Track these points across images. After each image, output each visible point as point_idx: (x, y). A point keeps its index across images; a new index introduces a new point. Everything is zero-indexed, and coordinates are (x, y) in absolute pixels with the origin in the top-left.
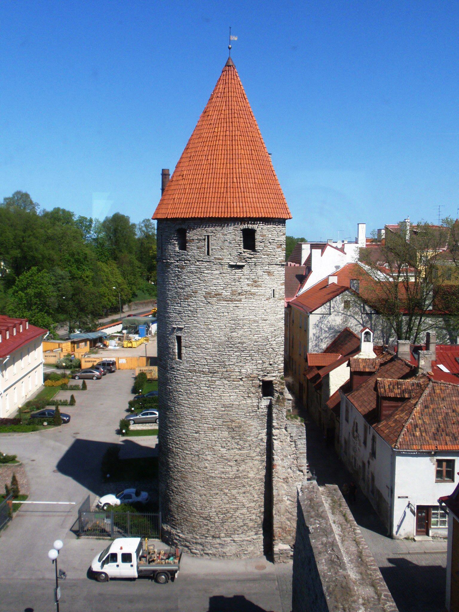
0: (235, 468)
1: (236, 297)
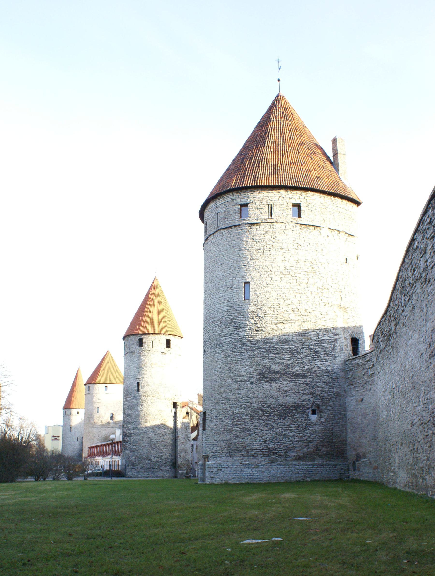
0: (162, 437)
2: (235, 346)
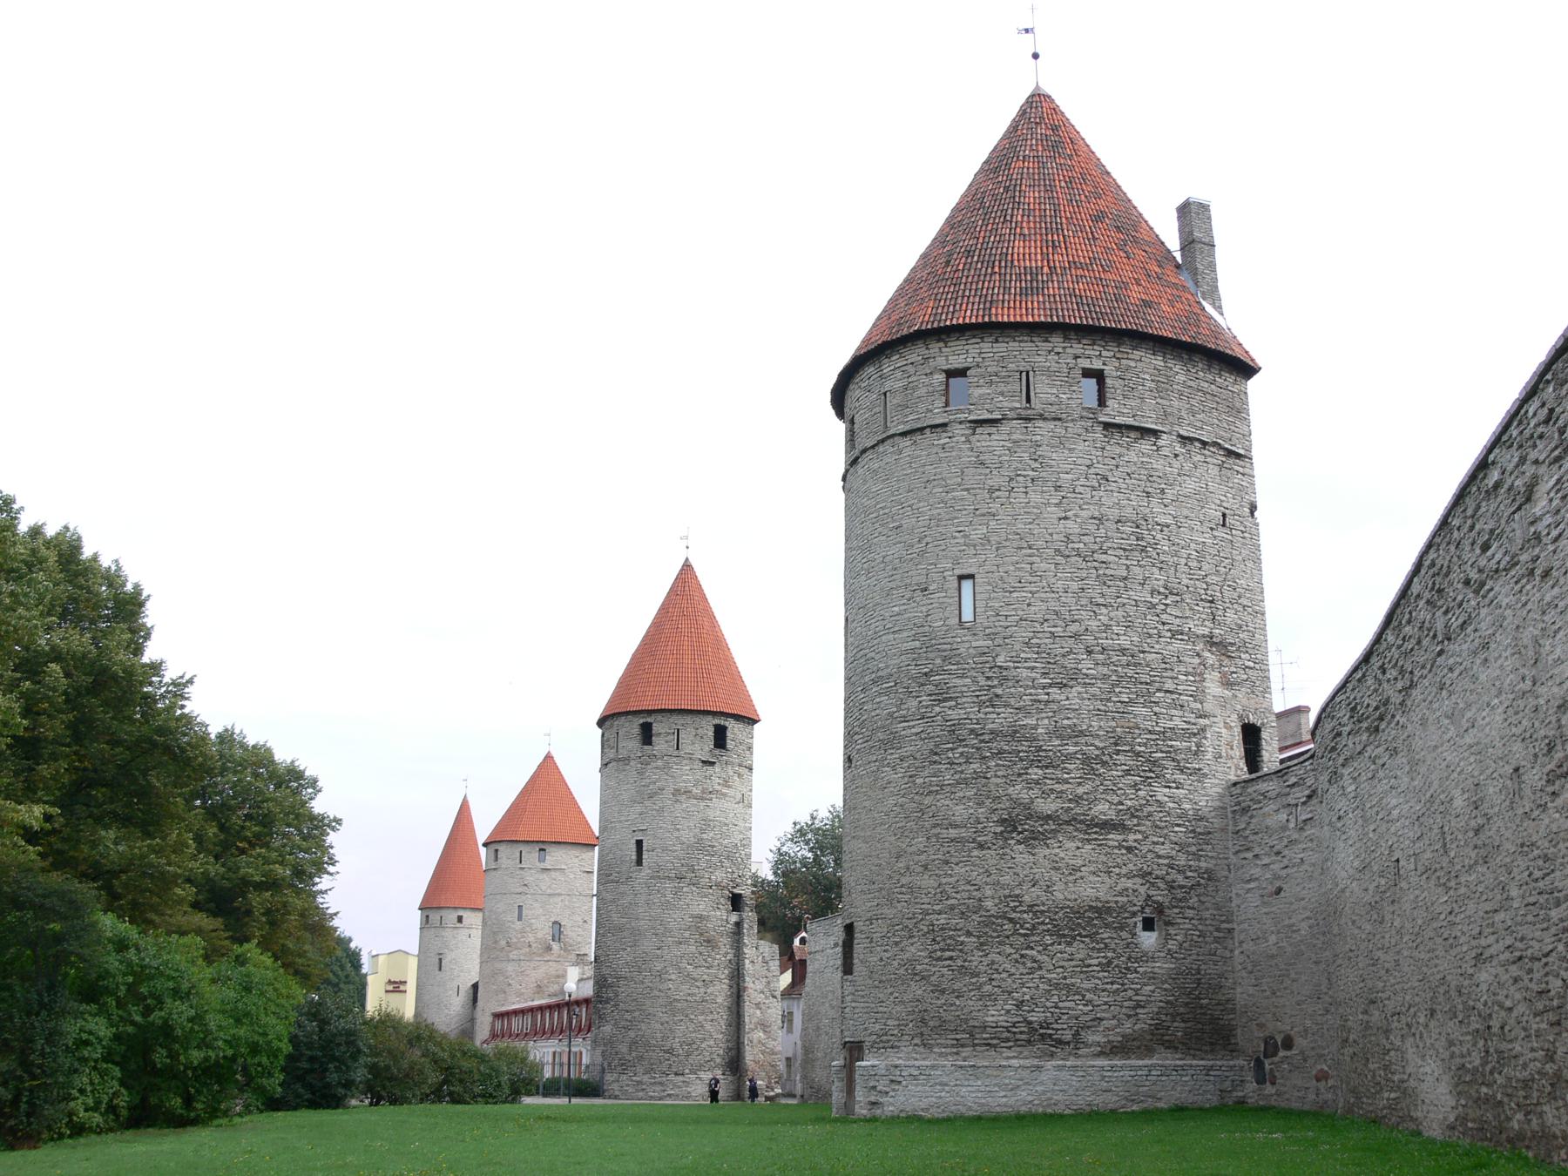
1: (706, 795)
2: (937, 746)
